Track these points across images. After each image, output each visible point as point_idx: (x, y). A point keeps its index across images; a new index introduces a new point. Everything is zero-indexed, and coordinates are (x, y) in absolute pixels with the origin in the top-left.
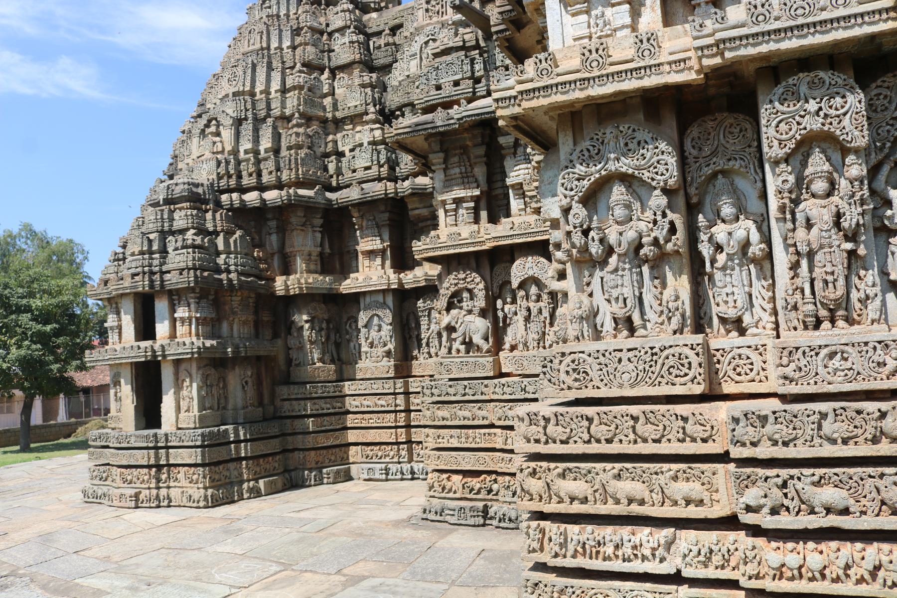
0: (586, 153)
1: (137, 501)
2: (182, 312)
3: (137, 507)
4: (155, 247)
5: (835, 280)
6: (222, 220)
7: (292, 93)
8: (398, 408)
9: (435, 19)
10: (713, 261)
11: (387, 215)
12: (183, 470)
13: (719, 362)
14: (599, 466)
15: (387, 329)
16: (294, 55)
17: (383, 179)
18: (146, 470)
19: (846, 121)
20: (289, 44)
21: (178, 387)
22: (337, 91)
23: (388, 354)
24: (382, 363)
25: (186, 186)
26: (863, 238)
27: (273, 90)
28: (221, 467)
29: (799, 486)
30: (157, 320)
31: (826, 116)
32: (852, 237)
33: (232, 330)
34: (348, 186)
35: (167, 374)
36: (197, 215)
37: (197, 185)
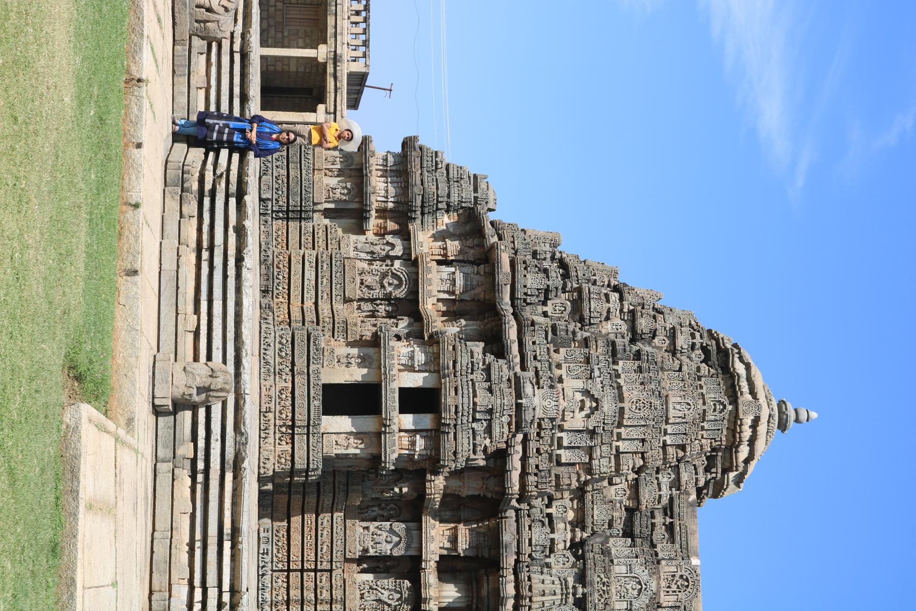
2: (420, 443)
7: (613, 464)
8: (319, 563)
9: (663, 584)
11: (486, 556)
12: (288, 448)
15: (386, 549)
17: (518, 557)
20: (669, 442)
21: (358, 435)
22: (613, 488)
23: (366, 550)
24: (358, 546)
27: (620, 443)
30: (416, 415)
34: (517, 521)
35: (368, 423)
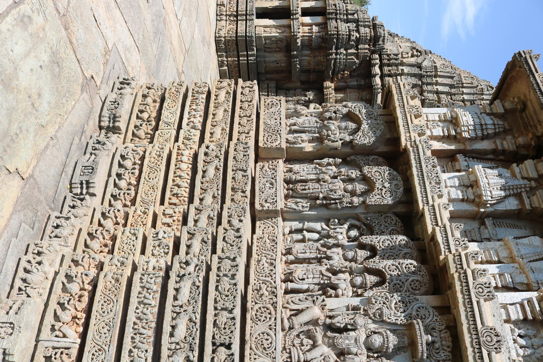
0: (371, 113)
1: (221, 5)
2: (315, 29)
3: (217, 5)
4: (350, 17)
5: (305, 190)
6: (365, 53)
10: (319, 164)
12: (235, 27)
13: (272, 162)
14: (231, 104)
16: (459, 101)
18: (235, 9)
19: (378, 197)
20: (466, 98)
25: (383, 35)
26: (325, 202)
27: (438, 87)
28: (235, 46)
29: (216, 161)
31: (381, 190)
32: (324, 198)
33: (306, 56)
35: (284, 22)
36: (367, 39)
37: (383, 41)
